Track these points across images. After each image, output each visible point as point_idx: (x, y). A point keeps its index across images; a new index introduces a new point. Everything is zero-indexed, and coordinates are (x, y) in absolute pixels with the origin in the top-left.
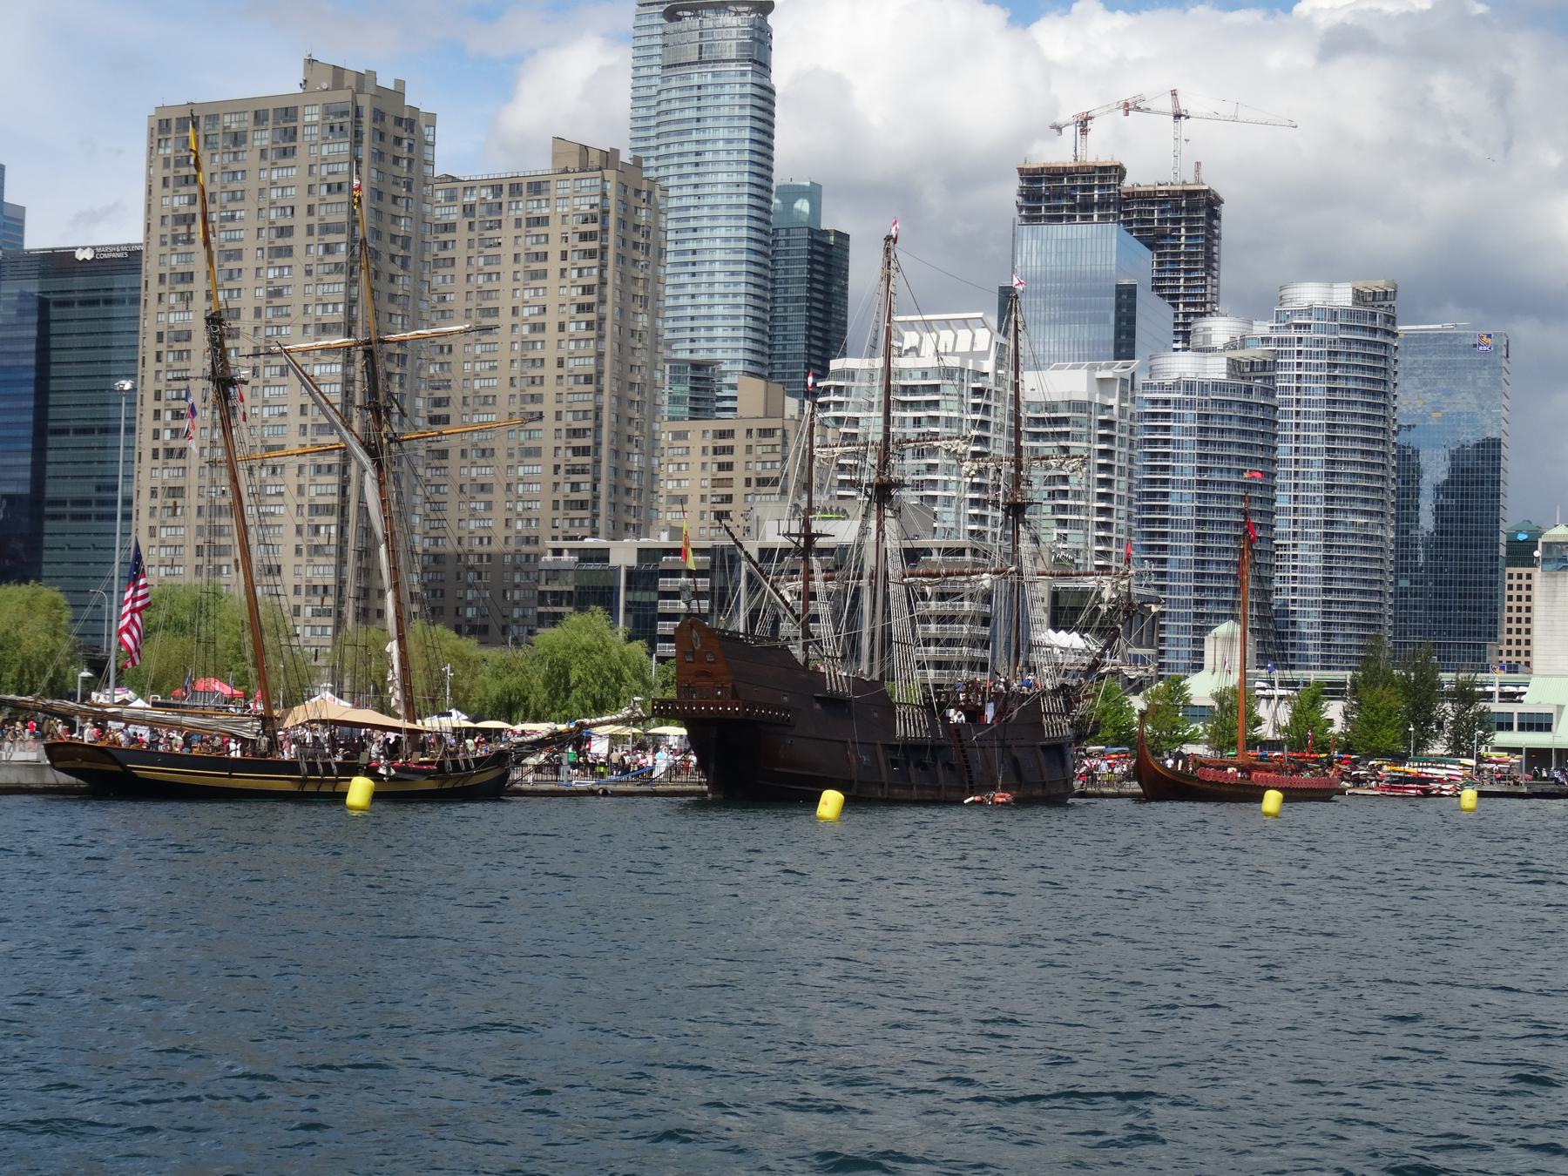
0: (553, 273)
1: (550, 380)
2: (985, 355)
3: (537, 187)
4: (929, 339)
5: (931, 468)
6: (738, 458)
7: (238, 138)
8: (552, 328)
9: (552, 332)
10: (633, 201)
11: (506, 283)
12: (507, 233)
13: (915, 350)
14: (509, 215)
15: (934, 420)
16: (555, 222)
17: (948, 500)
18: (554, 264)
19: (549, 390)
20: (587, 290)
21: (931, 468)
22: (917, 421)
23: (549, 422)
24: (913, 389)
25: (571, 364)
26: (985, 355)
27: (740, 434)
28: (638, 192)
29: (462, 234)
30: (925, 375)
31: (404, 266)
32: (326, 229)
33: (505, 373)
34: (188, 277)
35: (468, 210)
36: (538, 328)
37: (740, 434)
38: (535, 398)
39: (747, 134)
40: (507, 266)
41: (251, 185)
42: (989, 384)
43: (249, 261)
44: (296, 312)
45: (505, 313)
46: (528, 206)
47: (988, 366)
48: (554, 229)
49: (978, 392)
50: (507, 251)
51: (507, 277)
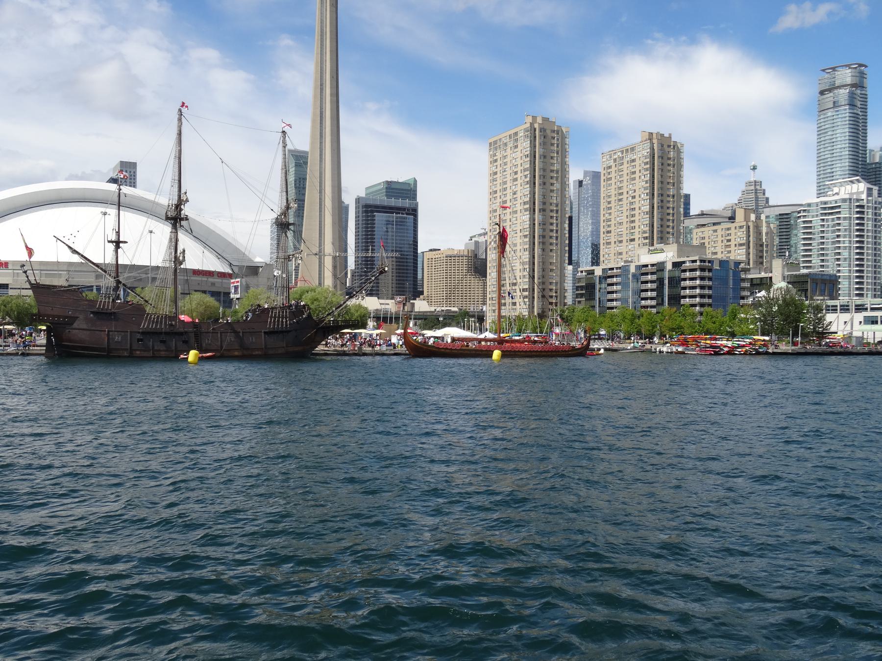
0: (637, 178)
1: (637, 215)
2: (862, 193)
3: (633, 149)
4: (843, 189)
5: (838, 236)
6: (732, 237)
7: (506, 144)
8: (637, 197)
10: (667, 149)
11: (625, 184)
12: (625, 165)
13: (837, 194)
14: (625, 161)
15: (839, 218)
16: (637, 160)
17: (845, 247)
18: (637, 175)
19: (636, 218)
20: (647, 182)
21: (838, 236)
22: (833, 220)
23: (637, 230)
24: (832, 208)
26: (862, 193)
27: (733, 229)
28: (669, 146)
29: (613, 169)
30: (836, 202)
31: (557, 180)
32: (525, 170)
33: (625, 214)
34: (496, 192)
35: (615, 160)
36: (634, 197)
37: (733, 229)
38: (633, 222)
39: (847, 130)
40: (625, 178)
41: (508, 160)
42: (865, 203)
43: (508, 185)
44: (519, 199)
45: (625, 193)
46: (631, 156)
47: (864, 196)
48: (637, 163)
49: (858, 206)
50: (625, 172)
51: (625, 181)
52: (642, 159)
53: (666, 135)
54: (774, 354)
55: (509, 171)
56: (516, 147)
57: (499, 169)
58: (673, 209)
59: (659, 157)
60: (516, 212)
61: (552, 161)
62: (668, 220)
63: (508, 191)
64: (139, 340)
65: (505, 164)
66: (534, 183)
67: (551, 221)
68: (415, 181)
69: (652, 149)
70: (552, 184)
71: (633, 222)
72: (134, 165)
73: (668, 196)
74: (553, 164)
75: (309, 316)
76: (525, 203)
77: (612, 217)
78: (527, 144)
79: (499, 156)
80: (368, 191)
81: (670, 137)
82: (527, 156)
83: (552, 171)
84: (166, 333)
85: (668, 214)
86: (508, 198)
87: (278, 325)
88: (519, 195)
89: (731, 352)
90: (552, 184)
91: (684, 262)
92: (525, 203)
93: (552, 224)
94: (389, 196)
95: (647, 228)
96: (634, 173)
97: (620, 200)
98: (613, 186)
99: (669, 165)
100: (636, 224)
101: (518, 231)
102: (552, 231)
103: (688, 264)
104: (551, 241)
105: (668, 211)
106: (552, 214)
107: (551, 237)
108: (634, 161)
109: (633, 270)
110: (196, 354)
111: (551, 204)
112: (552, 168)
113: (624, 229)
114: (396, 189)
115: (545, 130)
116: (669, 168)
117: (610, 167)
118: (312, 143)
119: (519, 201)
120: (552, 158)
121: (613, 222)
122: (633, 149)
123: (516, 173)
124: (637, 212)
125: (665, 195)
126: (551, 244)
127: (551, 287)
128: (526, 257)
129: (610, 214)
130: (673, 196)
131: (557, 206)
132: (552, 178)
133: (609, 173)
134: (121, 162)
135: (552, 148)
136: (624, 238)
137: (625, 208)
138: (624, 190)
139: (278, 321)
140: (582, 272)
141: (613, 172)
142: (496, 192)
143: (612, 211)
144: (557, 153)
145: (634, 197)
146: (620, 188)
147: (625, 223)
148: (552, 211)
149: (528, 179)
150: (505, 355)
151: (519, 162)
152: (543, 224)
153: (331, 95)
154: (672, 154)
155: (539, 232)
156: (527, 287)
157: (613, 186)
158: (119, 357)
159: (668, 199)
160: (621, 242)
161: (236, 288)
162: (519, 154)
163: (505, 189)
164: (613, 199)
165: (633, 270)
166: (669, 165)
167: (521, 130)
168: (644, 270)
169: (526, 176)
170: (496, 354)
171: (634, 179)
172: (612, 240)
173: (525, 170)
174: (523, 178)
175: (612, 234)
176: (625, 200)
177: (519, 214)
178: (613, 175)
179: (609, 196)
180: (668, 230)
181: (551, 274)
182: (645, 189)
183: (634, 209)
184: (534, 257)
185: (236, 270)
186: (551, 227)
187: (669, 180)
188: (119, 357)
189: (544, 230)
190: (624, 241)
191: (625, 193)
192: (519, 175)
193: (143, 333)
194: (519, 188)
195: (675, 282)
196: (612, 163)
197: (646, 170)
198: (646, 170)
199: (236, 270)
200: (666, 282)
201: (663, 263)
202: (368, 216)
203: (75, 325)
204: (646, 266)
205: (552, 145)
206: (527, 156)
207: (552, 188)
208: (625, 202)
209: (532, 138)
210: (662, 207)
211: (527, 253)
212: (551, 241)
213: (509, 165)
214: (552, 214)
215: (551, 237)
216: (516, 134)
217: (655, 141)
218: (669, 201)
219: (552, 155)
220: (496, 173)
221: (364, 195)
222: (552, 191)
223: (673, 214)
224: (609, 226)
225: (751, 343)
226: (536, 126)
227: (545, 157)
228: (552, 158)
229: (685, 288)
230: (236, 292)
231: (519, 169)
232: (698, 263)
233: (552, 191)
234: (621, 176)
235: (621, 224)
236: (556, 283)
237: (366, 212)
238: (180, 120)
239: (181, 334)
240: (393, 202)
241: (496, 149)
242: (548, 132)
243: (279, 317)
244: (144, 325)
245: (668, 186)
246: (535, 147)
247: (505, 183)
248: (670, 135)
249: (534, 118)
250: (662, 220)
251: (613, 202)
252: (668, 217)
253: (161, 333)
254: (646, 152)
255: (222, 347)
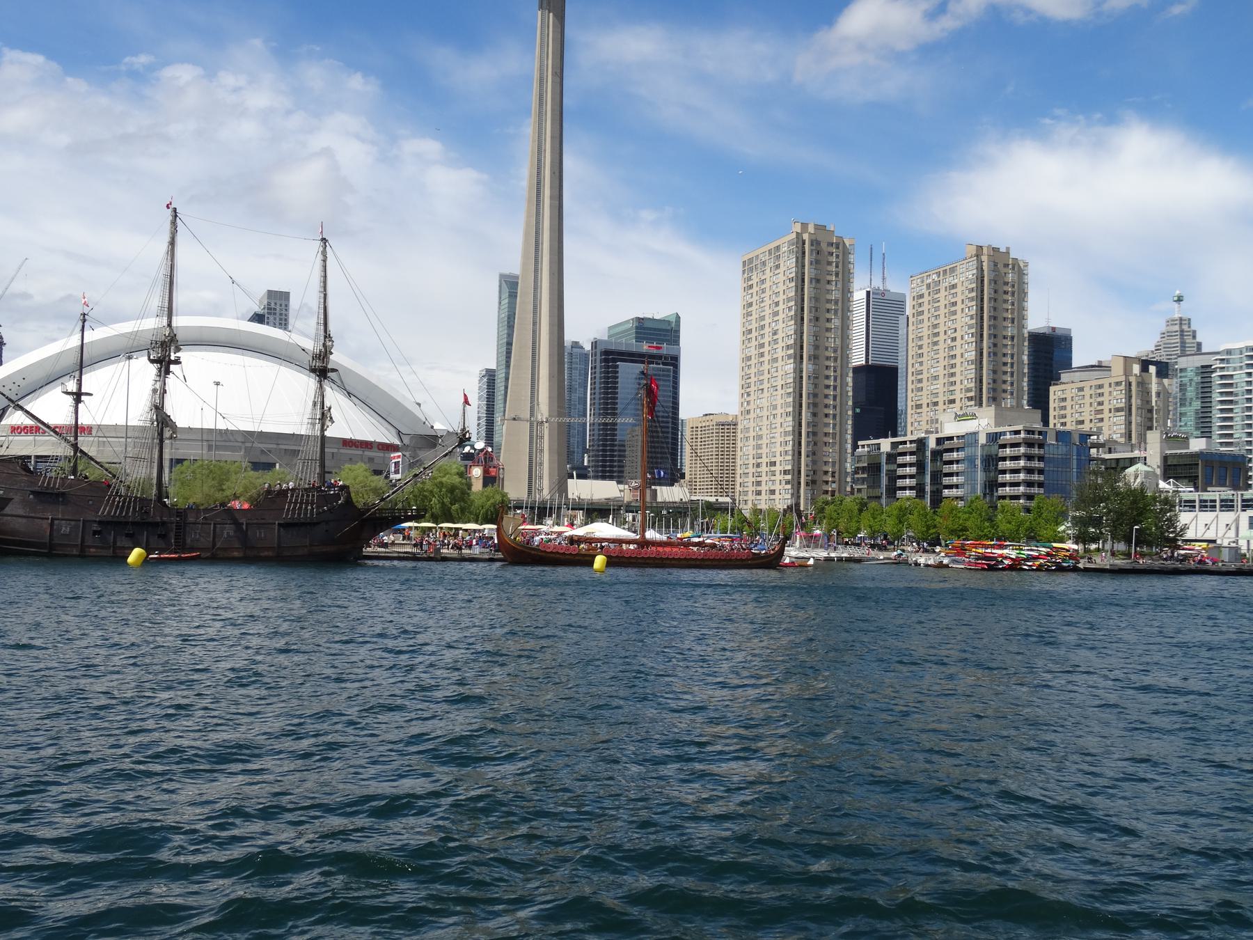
0: (959, 312)
1: (958, 365)
7: (764, 263)
8: (959, 339)
9: (959, 341)
10: (1003, 270)
11: (942, 320)
12: (943, 293)
14: (942, 286)
18: (959, 307)
19: (957, 370)
20: (972, 317)
23: (958, 387)
25: (966, 355)
27: (1106, 386)
28: (1006, 265)
29: (926, 299)
32: (789, 300)
33: (942, 363)
34: (750, 331)
36: (954, 339)
37: (1106, 386)
38: (953, 375)
40: (942, 311)
41: (767, 285)
45: (942, 334)
46: (951, 280)
48: (959, 290)
50: (942, 304)
51: (942, 316)
52: (966, 284)
53: (1003, 250)
54: (1086, 570)
55: (768, 302)
56: (778, 267)
57: (755, 298)
58: (1012, 356)
59: (990, 281)
60: (775, 360)
61: (828, 287)
62: (1005, 373)
63: (767, 330)
64: (95, 533)
65: (763, 291)
66: (802, 319)
67: (827, 373)
68: (678, 318)
69: (980, 269)
70: (828, 320)
71: (953, 375)
72: (285, 296)
73: (1005, 337)
74: (829, 292)
75: (349, 501)
76: (788, 347)
77: (924, 368)
78: (792, 262)
79: (755, 280)
80: (612, 332)
81: (1008, 253)
82: (791, 280)
83: (829, 301)
84: (134, 523)
85: (1005, 364)
86: (766, 340)
87: (299, 514)
88: (780, 335)
89: (1016, 566)
90: (828, 320)
91: (1004, 433)
92: (788, 347)
93: (827, 377)
94: (639, 338)
95: (973, 385)
96: (954, 304)
97: (935, 343)
98: (926, 324)
99: (1006, 293)
100: (957, 378)
101: (779, 388)
102: (828, 387)
103: (1008, 436)
104: (826, 401)
105: (1004, 360)
106: (827, 363)
107: (826, 396)
108: (954, 286)
109: (932, 444)
110: (140, 555)
111: (827, 349)
112: (828, 297)
113: (939, 386)
114: (650, 329)
115: (818, 243)
116: (1006, 297)
117: (921, 296)
118: (524, 265)
119: (781, 344)
120: (829, 282)
121: (925, 376)
122: (953, 270)
123: (777, 304)
124: (958, 361)
125: (1000, 337)
126: (826, 406)
127: (825, 468)
128: (789, 423)
129: (921, 364)
130: (1012, 338)
131: (835, 351)
132: (828, 311)
133: (920, 305)
134: (269, 292)
135: (829, 268)
136: (941, 399)
137: (942, 355)
138: (941, 329)
139: (300, 508)
140: (863, 446)
141: (926, 304)
142: (750, 331)
143: (924, 359)
144: (837, 275)
145: (954, 339)
146: (935, 326)
147: (941, 377)
148: (828, 358)
149: (793, 313)
150: (612, 562)
151: (781, 288)
152: (815, 377)
153: (552, 198)
154: (1010, 277)
155: (808, 388)
156: (789, 467)
157: (926, 324)
158: (66, 556)
159: (1005, 342)
160: (936, 404)
161: (397, 464)
162: (781, 278)
163: (763, 327)
164: (925, 342)
165: (932, 444)
166: (1006, 293)
167: (785, 241)
168: (947, 444)
169: (790, 309)
170: (599, 561)
171: (955, 313)
172: (924, 402)
173: (789, 300)
174: (786, 311)
175: (925, 392)
176: (941, 343)
177: (780, 363)
178: (925, 308)
179: (920, 338)
180: (1004, 387)
181: (825, 449)
182: (970, 327)
183: (954, 357)
184: (800, 425)
185: (406, 440)
186: (827, 382)
187: (1005, 315)
188: (66, 556)
189: (816, 385)
190: (941, 404)
191: (942, 334)
192: (781, 307)
193: (100, 523)
194: (781, 325)
195: (991, 461)
196: (924, 290)
197: (971, 299)
198: (971, 299)
199: (406, 440)
200: (978, 462)
201: (975, 434)
202: (608, 367)
203: (8, 510)
204: (951, 438)
205: (830, 263)
206: (791, 280)
207: (828, 325)
208: (941, 346)
209: (800, 255)
210: (995, 354)
211: (790, 418)
212: (826, 401)
213: (768, 293)
214: (827, 363)
215: (826, 396)
216: (778, 248)
217: (985, 258)
218: (1006, 346)
219: (829, 278)
220: (750, 305)
221: (606, 338)
222: (828, 330)
223: (1012, 364)
224: (920, 381)
225: (1048, 554)
226: (806, 237)
227: (818, 281)
228: (829, 282)
229: (1004, 472)
230: (397, 472)
231: (781, 297)
232: (1022, 435)
233: (828, 330)
234: (937, 309)
235: (936, 378)
236: (834, 463)
237: (606, 361)
238: (174, 223)
239: (156, 525)
240: (645, 347)
241: (751, 270)
242: (824, 245)
243: (301, 503)
244: (104, 511)
245: (1005, 324)
246: (803, 266)
247: (762, 318)
248: (1008, 248)
249: (804, 226)
250: (995, 372)
251: (925, 347)
252: (1005, 369)
253: (127, 523)
254: (971, 273)
255: (214, 544)
